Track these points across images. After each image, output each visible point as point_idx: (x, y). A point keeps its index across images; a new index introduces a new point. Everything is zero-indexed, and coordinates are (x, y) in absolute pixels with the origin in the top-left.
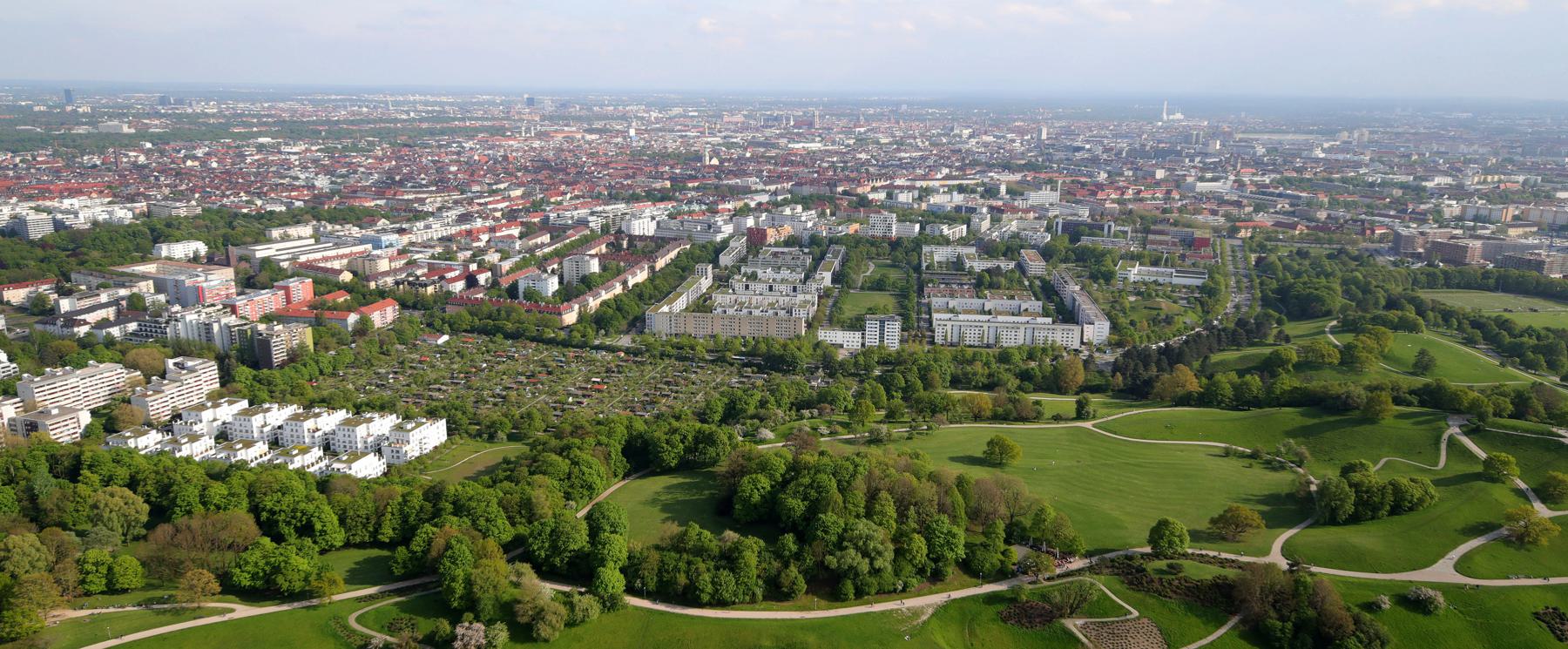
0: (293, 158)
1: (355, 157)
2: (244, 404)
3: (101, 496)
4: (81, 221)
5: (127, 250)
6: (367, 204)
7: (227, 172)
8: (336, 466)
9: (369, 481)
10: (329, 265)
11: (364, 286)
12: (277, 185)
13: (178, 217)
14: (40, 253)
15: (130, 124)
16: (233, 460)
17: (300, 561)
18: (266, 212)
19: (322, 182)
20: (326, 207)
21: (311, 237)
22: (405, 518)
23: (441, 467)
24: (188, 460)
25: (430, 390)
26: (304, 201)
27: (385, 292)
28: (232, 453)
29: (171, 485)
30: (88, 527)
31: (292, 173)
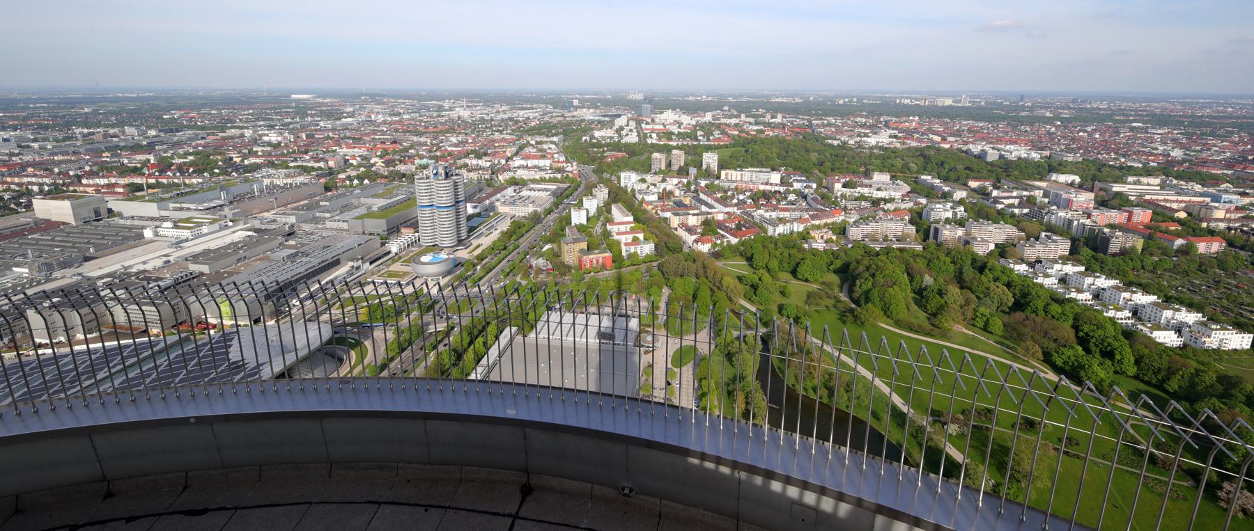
0: (1156, 136)
1: (1210, 140)
2: (1082, 269)
3: (992, 285)
4: (1012, 157)
5: (1033, 173)
6: (1213, 172)
7: (1105, 141)
8: (1140, 327)
9: (1166, 347)
10: (1168, 205)
11: (1195, 224)
12: (1139, 152)
13: (1067, 161)
14: (990, 168)
15: (1051, 112)
16: (1067, 296)
17: (1100, 370)
18: (1127, 166)
19: (1177, 153)
20: (1176, 169)
21: (1158, 185)
22: (1193, 385)
23: (1236, 365)
24: (1041, 286)
25: (1241, 309)
26: (1158, 163)
27: (1215, 231)
28: (1067, 292)
29: (1029, 294)
30: (982, 296)
31: (1153, 145)
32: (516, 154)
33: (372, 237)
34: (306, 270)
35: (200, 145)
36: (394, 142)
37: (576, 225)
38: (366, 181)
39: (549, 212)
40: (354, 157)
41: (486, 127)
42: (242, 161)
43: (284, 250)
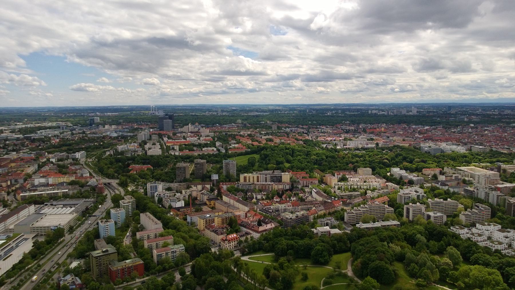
39: (71, 230)
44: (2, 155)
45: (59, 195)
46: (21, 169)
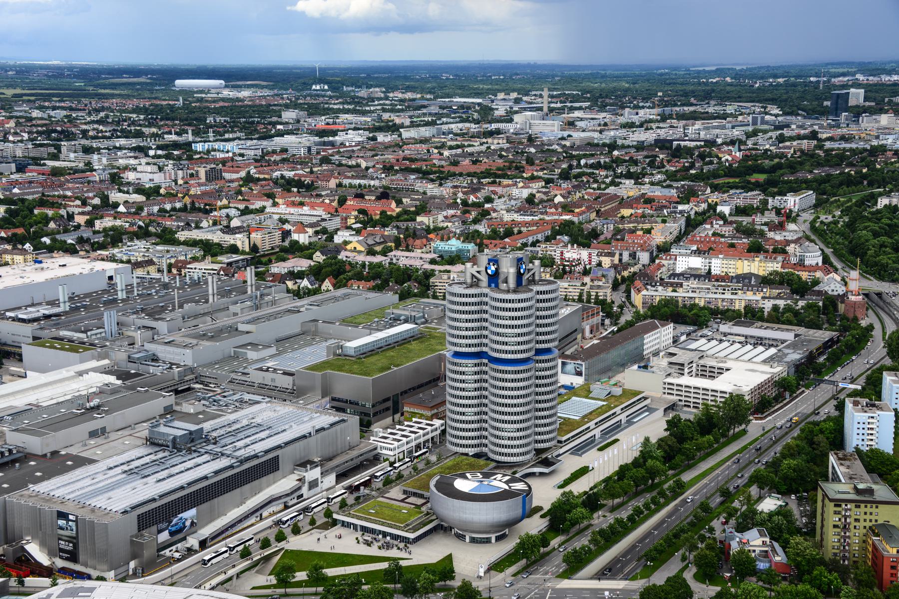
32: (678, 239)
33: (343, 416)
34: (216, 473)
35: (15, 183)
36: (384, 195)
37: (858, 451)
38: (327, 284)
40: (301, 227)
41: (598, 166)
42: (90, 223)
43: (177, 424)
44: (603, 186)
45: (737, 308)
46: (647, 226)
